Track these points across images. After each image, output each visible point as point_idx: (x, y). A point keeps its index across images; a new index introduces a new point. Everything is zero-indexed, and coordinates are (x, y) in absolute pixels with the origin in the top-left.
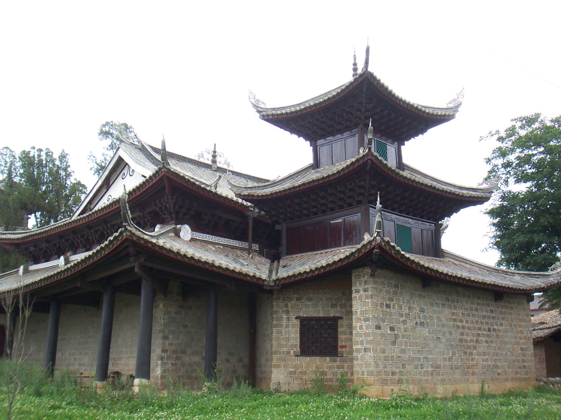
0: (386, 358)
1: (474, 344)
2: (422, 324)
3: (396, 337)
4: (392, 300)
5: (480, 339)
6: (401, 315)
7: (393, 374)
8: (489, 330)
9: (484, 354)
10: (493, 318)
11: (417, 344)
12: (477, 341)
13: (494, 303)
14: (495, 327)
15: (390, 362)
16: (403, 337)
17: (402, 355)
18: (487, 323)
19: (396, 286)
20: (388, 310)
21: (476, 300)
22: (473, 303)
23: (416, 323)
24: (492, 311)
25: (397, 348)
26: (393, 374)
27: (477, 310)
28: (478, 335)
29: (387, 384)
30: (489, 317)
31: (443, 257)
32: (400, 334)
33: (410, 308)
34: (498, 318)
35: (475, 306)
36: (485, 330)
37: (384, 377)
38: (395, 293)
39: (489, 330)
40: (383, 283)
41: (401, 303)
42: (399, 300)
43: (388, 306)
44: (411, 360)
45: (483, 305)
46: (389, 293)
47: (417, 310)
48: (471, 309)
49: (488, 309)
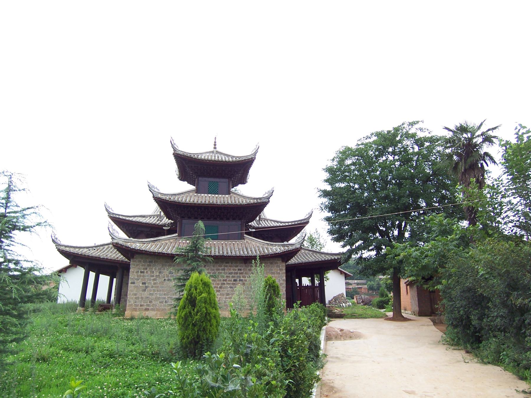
0: (136, 298)
1: (218, 289)
2: (169, 280)
3: (146, 287)
4: (147, 269)
5: (223, 286)
6: (153, 276)
7: (141, 306)
8: (235, 280)
9: (228, 294)
10: (242, 273)
11: (163, 291)
12: (220, 287)
13: (244, 265)
14: (242, 278)
15: (140, 300)
16: (152, 287)
17: (150, 297)
18: (233, 277)
19: (150, 262)
20: (142, 274)
21: (224, 264)
22: (221, 266)
23: (165, 280)
24: (241, 270)
25: (146, 294)
26: (141, 306)
27: (224, 269)
28: (224, 284)
29: (136, 311)
30: (237, 273)
31: (244, 239)
32: (150, 286)
33: (160, 272)
34: (246, 273)
35: (223, 268)
36: (231, 281)
37: (134, 307)
38: (149, 266)
39: (235, 280)
40: (140, 261)
41: (154, 270)
42: (152, 269)
43: (141, 272)
44: (157, 299)
45: (231, 266)
46: (145, 265)
47: (167, 273)
48: (218, 270)
49: (237, 268)
